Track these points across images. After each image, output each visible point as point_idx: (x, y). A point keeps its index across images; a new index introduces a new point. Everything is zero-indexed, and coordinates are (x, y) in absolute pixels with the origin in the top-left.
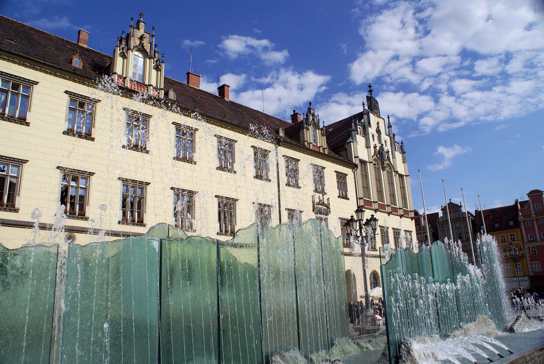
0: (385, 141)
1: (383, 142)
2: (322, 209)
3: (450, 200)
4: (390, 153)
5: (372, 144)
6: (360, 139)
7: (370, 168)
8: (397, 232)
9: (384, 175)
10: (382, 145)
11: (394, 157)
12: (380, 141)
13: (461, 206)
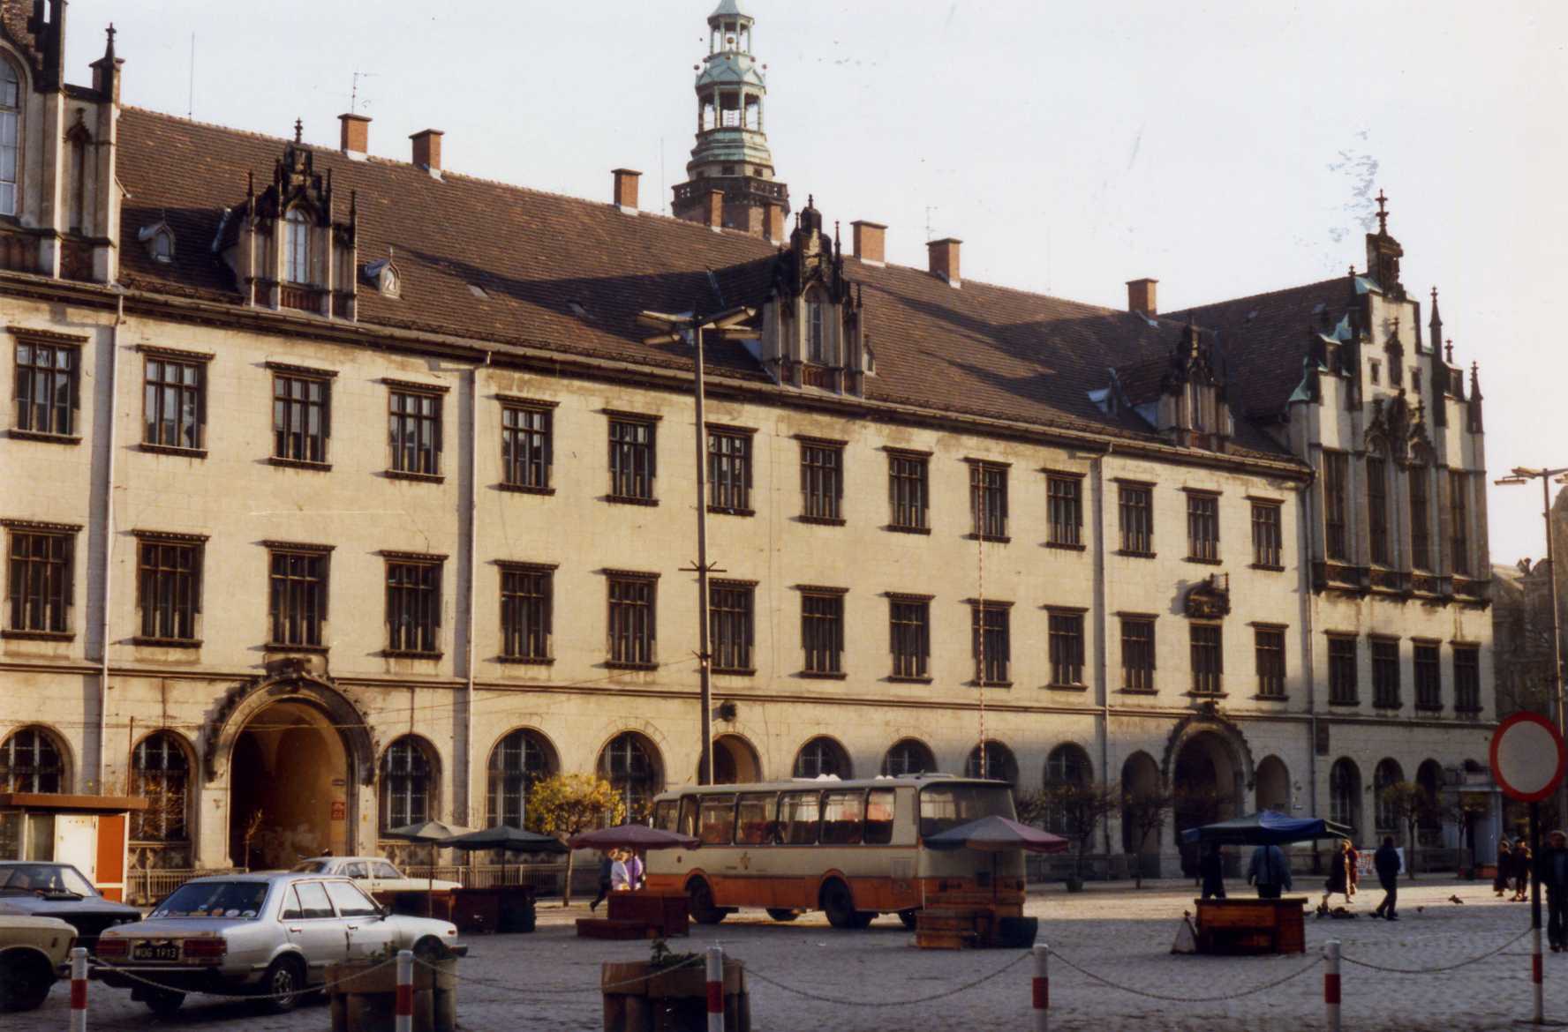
4: (1428, 413)
5: (1368, 392)
6: (1329, 386)
10: (1402, 392)
12: (1396, 378)
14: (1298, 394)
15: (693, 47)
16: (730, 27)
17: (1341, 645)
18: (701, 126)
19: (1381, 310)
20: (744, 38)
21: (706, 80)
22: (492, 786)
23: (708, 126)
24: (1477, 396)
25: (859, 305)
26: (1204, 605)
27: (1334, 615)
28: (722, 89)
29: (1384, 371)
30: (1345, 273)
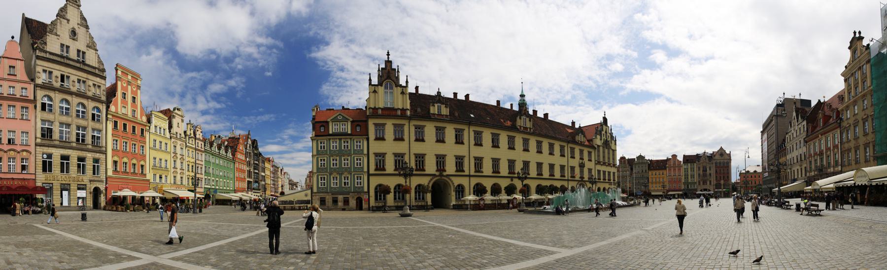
2: (582, 166)
8: (609, 173)
17: (599, 171)
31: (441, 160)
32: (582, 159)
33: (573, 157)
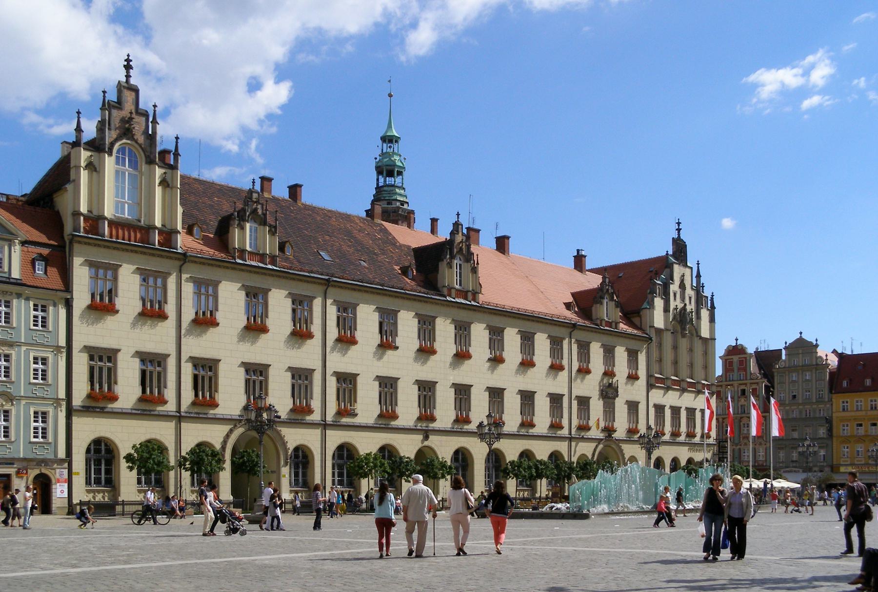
0: (690, 298)
1: (687, 302)
3: (801, 333)
5: (672, 305)
6: (659, 303)
7: (668, 339)
9: (684, 343)
11: (699, 317)
13: (817, 346)
14: (645, 305)
15: (374, 149)
16: (391, 141)
17: (659, 409)
18: (378, 184)
19: (678, 270)
20: (396, 146)
21: (380, 164)
22: (333, 468)
23: (380, 184)
24: (713, 307)
25: (478, 264)
26: (609, 393)
27: (657, 396)
28: (387, 170)
29: (678, 296)
30: (664, 254)
31: (256, 375)
32: (609, 374)
33: (584, 371)
